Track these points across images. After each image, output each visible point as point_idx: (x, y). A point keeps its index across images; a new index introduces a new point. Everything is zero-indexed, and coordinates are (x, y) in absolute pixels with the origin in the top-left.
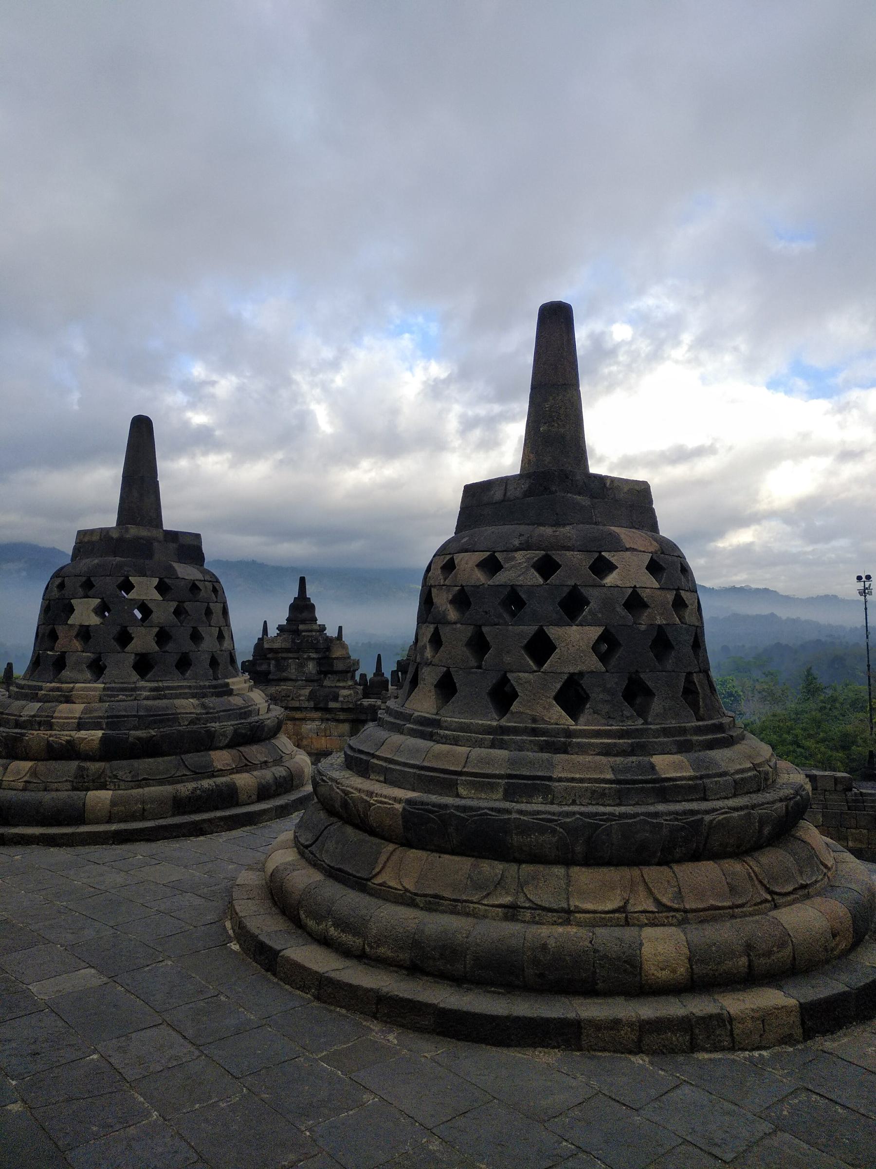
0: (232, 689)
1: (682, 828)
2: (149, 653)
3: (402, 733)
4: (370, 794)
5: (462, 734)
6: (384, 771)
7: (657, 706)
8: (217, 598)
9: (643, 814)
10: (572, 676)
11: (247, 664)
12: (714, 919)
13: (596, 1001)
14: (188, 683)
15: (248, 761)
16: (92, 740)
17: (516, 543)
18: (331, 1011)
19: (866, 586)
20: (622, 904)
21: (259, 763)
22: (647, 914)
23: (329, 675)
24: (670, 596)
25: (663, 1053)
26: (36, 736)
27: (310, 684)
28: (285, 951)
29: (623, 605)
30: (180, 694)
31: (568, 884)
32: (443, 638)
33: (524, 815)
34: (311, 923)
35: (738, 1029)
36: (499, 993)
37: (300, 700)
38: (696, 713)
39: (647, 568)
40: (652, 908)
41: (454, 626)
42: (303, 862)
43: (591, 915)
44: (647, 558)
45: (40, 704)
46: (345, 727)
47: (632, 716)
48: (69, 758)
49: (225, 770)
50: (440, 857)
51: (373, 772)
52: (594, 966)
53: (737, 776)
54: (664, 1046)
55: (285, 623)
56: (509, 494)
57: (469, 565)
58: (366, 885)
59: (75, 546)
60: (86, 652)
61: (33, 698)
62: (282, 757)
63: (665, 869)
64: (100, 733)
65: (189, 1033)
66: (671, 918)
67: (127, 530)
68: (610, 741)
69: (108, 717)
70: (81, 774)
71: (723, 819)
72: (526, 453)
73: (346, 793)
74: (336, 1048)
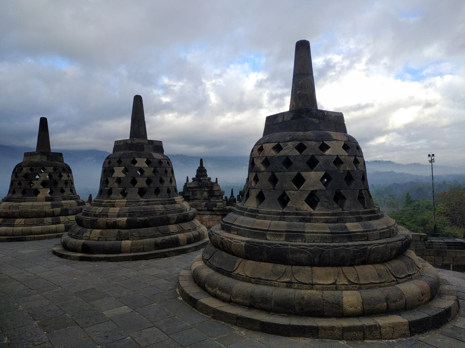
0: (176, 201)
1: (359, 251)
2: (144, 188)
3: (243, 216)
4: (232, 239)
5: (268, 215)
6: (237, 230)
7: (347, 203)
9: (342, 246)
10: (312, 191)
11: (181, 193)
12: (372, 288)
13: (324, 319)
14: (159, 199)
15: (182, 228)
16: (123, 221)
17: (288, 139)
18: (218, 323)
19: (432, 159)
20: (334, 281)
21: (187, 229)
22: (345, 286)
23: (213, 197)
24: (352, 159)
25: (352, 340)
26: (102, 220)
27: (206, 200)
28: (200, 300)
29: (333, 163)
30: (156, 203)
31: (312, 273)
32: (259, 178)
33: (294, 247)
34: (210, 289)
35: (383, 331)
36: (285, 316)
37: (201, 207)
38: (364, 206)
39: (342, 148)
40: (347, 283)
41: (263, 173)
42: (206, 266)
43: (322, 286)
44: (343, 144)
45: (103, 208)
46: (220, 217)
47: (337, 207)
48: (115, 228)
49: (174, 232)
50: (260, 263)
51: (232, 230)
52: (323, 306)
53: (381, 231)
54: (352, 337)
55: (195, 177)
56: (285, 119)
57: (269, 148)
58: (231, 274)
59: (114, 147)
60: (120, 188)
61: (100, 206)
62: (196, 227)
63: (352, 268)
64: (126, 219)
65: (164, 330)
66: (354, 287)
67: (134, 140)
68: (328, 217)
69: (129, 212)
70: (119, 234)
71: (376, 248)
72: (292, 102)
73: (222, 239)
74: (221, 336)
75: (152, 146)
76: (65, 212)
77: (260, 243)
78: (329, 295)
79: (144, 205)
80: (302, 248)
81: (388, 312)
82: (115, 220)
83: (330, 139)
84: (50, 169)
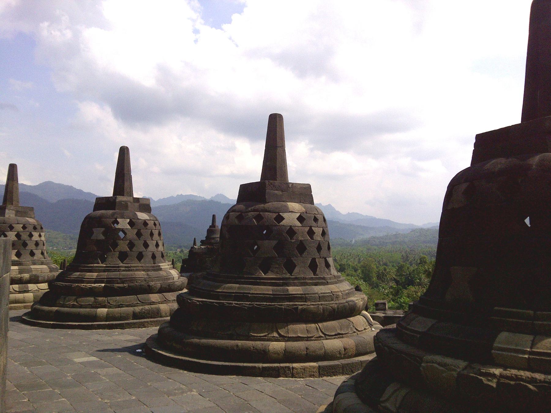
0: (162, 268)
8: (156, 227)
9: (276, 305)
49: (156, 302)
55: (205, 239)
64: (103, 285)
69: (107, 278)
75: (138, 204)
76: (35, 280)
79: (124, 271)
80: (243, 306)
82: (91, 286)
84: (19, 227)
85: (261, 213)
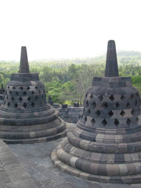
40: (32, 130)
44: (35, 86)
77: (8, 120)
78: (26, 133)
81: (43, 136)
83: (31, 85)
85: (22, 87)
